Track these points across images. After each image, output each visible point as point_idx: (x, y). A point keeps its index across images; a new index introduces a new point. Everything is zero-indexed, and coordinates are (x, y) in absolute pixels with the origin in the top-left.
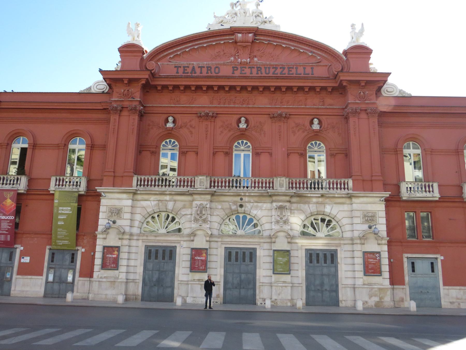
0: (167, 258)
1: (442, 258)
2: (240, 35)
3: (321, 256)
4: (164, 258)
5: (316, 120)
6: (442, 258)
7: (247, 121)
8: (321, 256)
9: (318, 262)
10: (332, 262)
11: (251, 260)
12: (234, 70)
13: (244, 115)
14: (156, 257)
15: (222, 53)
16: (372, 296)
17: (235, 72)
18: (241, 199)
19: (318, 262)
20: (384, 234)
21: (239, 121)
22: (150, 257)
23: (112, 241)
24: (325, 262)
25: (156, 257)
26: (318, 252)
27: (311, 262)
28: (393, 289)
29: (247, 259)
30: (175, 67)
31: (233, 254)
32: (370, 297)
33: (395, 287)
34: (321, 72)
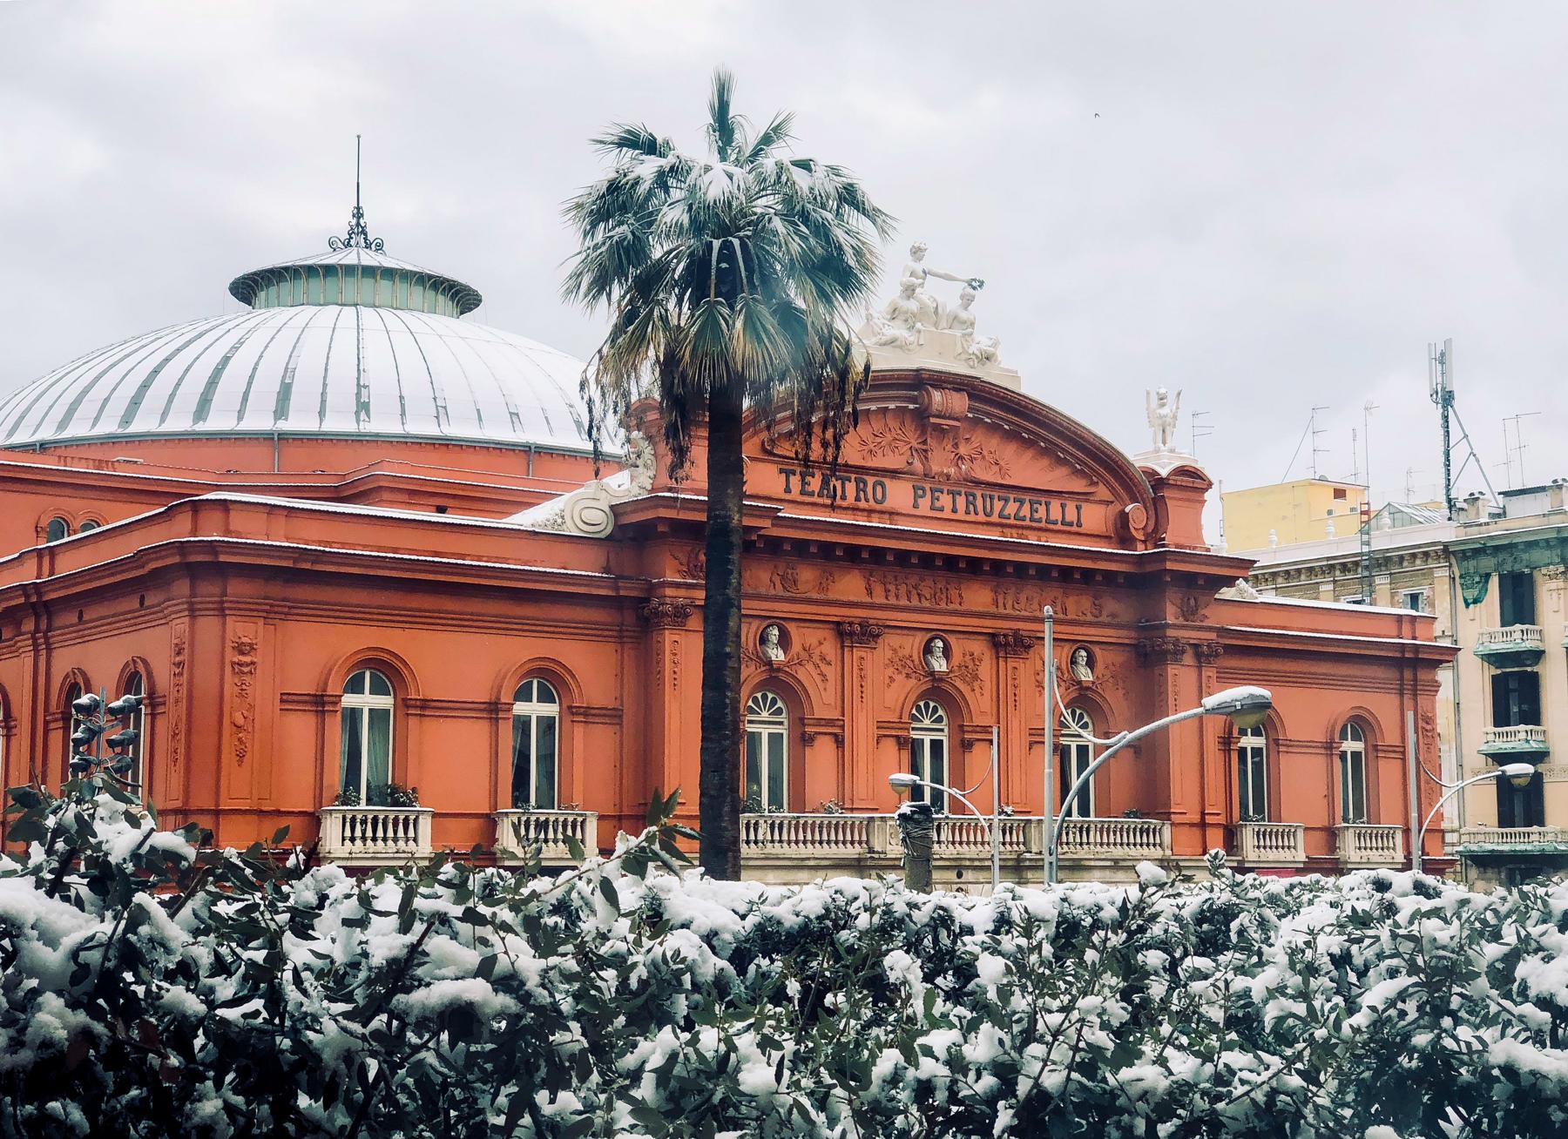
2: (937, 396)
5: (1084, 653)
7: (947, 652)
12: (916, 497)
13: (937, 634)
15: (889, 437)
18: (960, 875)
21: (928, 650)
30: (781, 471)
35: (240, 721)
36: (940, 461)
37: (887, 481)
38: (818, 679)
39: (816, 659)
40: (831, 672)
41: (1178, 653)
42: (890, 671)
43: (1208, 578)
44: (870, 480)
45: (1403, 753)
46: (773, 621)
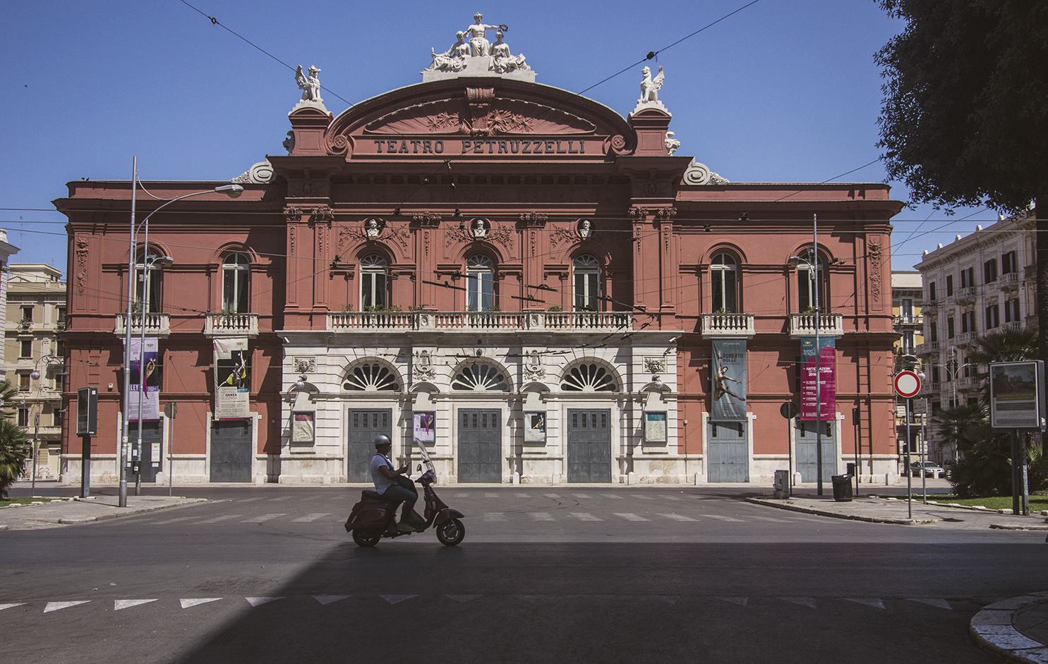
0: (380, 423)
1: (755, 417)
3: (589, 418)
4: (375, 425)
5: (587, 222)
6: (755, 417)
7: (487, 226)
8: (589, 418)
9: (584, 425)
10: (604, 426)
11: (494, 425)
14: (366, 425)
16: (653, 470)
17: (467, 149)
19: (584, 425)
20: (674, 389)
22: (356, 425)
23: (303, 402)
24: (594, 426)
25: (366, 425)
26: (584, 413)
27: (575, 425)
28: (686, 459)
29: (489, 423)
31: (471, 417)
32: (652, 469)
33: (689, 456)
34: (594, 149)
35: (81, 276)
36: (479, 126)
37: (444, 141)
38: (401, 245)
39: (400, 235)
40: (409, 242)
41: (640, 217)
42: (448, 239)
43: (670, 172)
44: (433, 142)
45: (855, 270)
46: (371, 217)
